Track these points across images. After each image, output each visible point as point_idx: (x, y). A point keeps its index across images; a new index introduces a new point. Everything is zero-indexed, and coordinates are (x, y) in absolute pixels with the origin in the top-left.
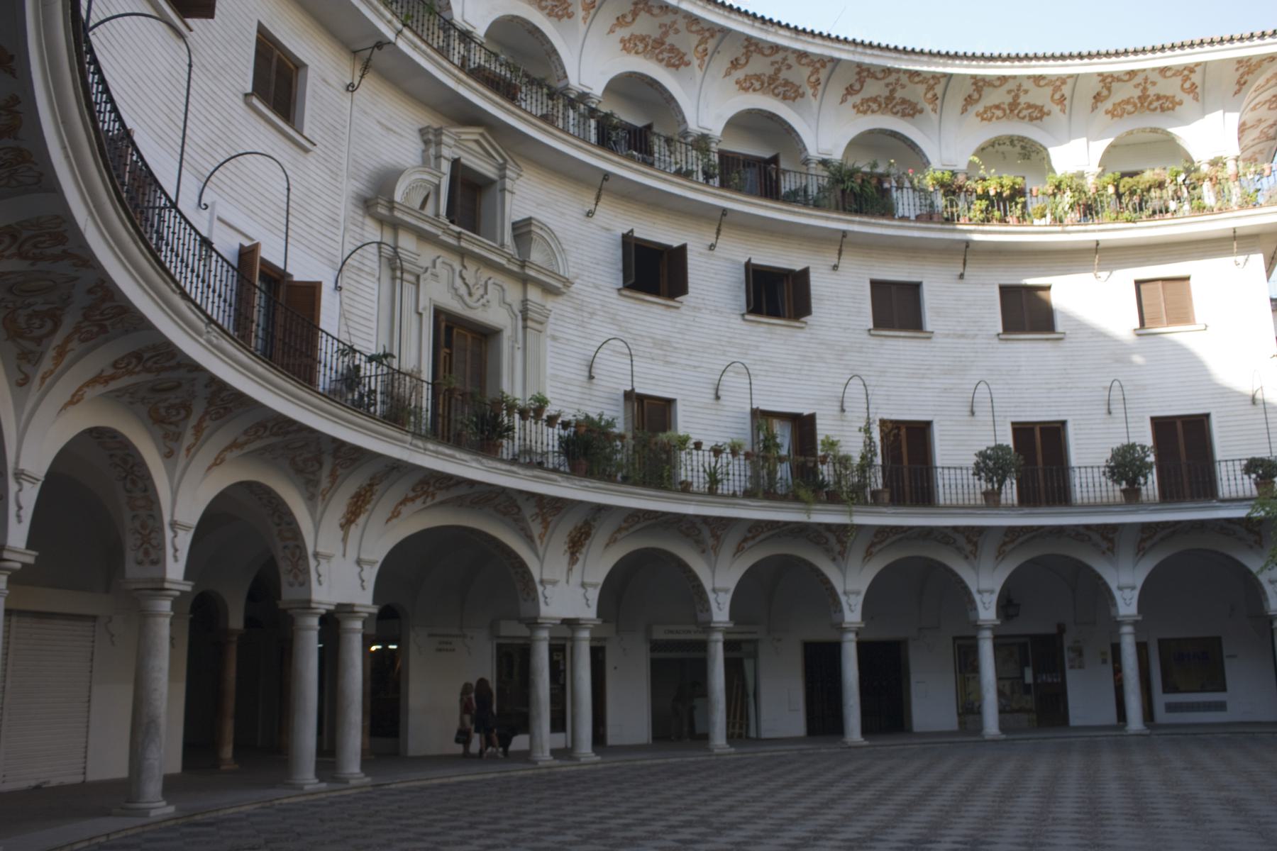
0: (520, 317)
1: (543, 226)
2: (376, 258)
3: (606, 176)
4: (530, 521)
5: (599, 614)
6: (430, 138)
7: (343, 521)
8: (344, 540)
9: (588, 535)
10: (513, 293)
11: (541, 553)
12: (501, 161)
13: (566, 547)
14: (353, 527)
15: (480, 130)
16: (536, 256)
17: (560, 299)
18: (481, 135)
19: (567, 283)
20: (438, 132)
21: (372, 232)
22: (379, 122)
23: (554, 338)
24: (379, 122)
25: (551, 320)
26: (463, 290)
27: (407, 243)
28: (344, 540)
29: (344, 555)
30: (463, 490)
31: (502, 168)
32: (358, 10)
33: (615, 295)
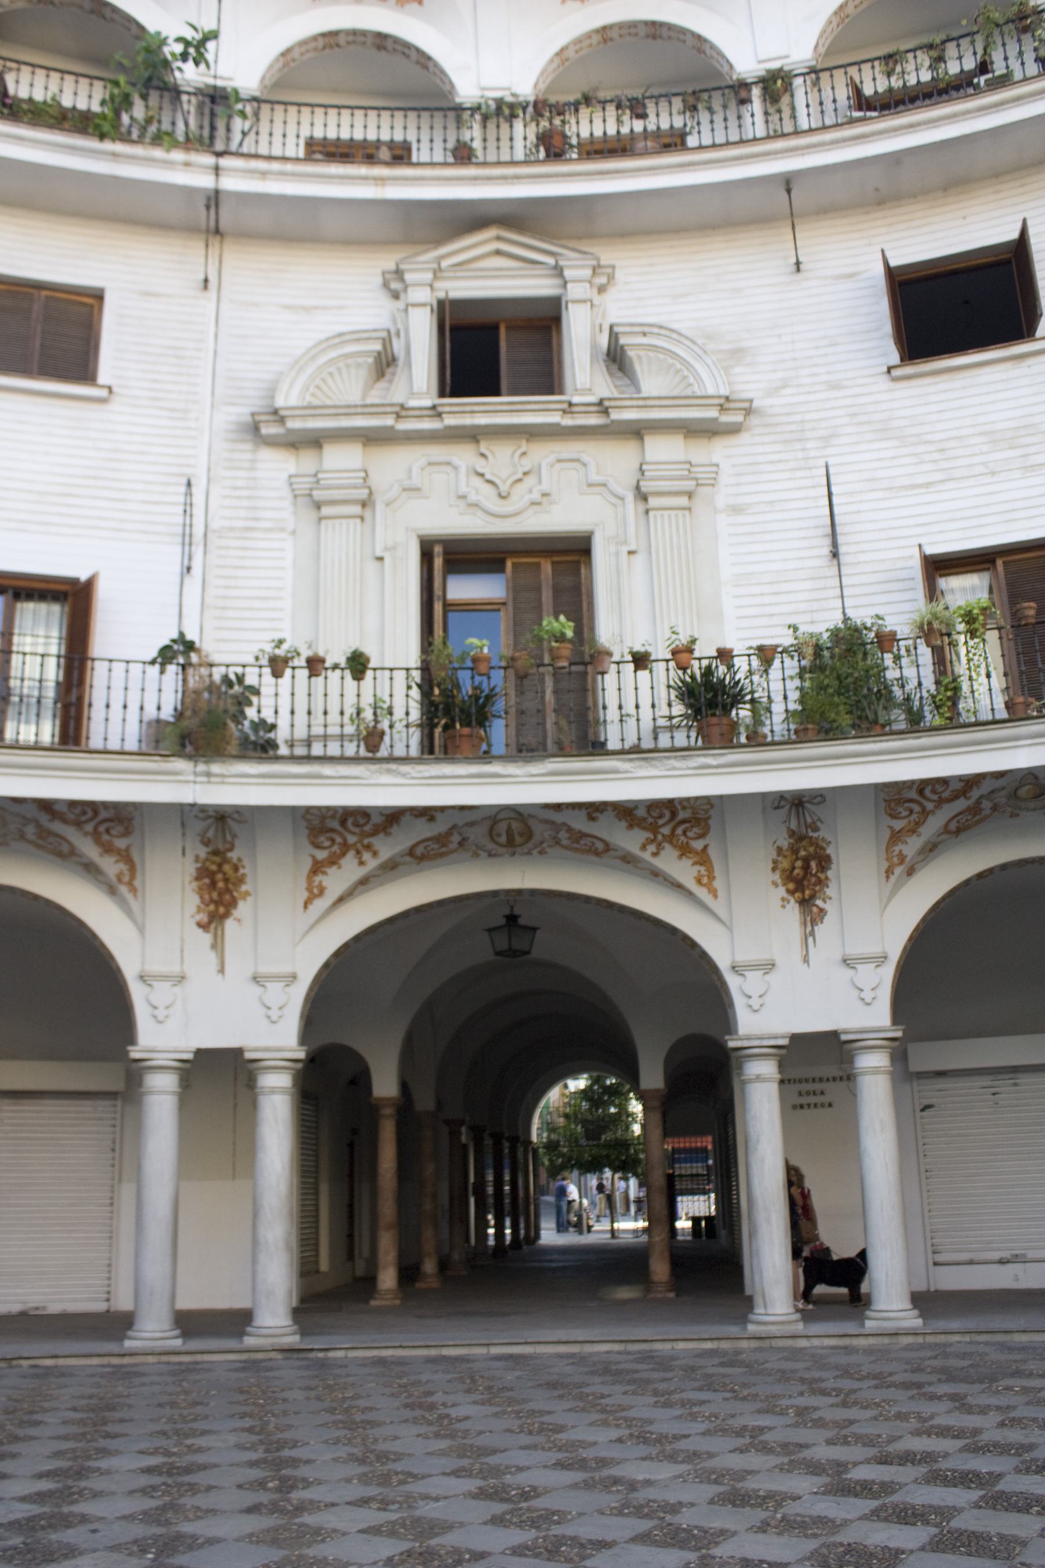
0: (630, 497)
1: (644, 330)
2: (287, 503)
3: (788, 182)
4: (646, 855)
5: (897, 1015)
6: (394, 285)
7: (203, 917)
8: (218, 945)
9: (824, 862)
10: (615, 461)
11: (722, 913)
12: (551, 261)
13: (782, 891)
14: (229, 924)
15: (492, 232)
16: (652, 382)
17: (744, 438)
18: (499, 238)
19: (725, 403)
20: (399, 274)
21: (278, 467)
22: (287, 307)
23: (736, 510)
24: (287, 307)
25: (724, 479)
26: (485, 495)
27: (342, 460)
28: (218, 945)
29: (222, 971)
30: (423, 830)
31: (558, 271)
32: (116, 178)
33: (884, 383)
